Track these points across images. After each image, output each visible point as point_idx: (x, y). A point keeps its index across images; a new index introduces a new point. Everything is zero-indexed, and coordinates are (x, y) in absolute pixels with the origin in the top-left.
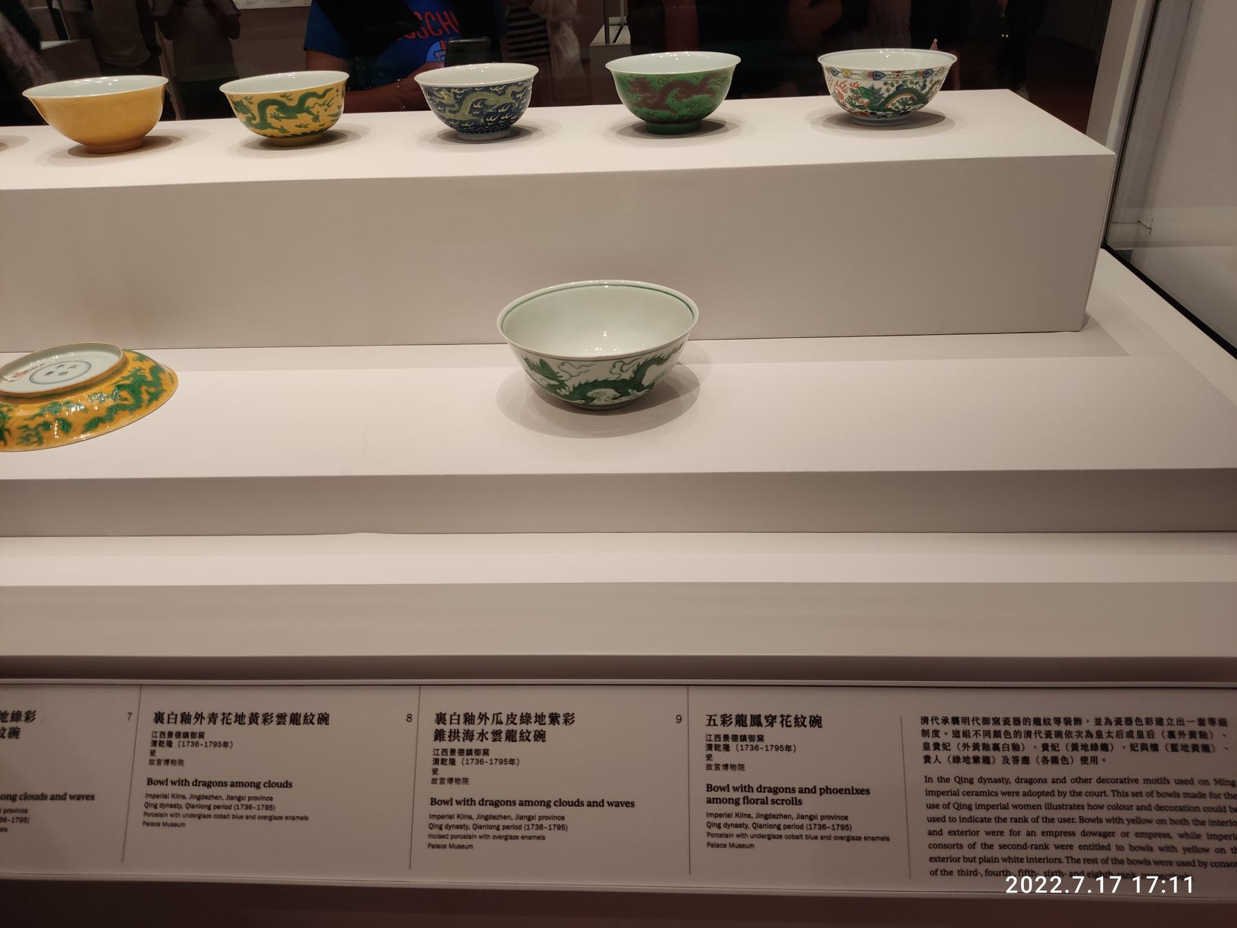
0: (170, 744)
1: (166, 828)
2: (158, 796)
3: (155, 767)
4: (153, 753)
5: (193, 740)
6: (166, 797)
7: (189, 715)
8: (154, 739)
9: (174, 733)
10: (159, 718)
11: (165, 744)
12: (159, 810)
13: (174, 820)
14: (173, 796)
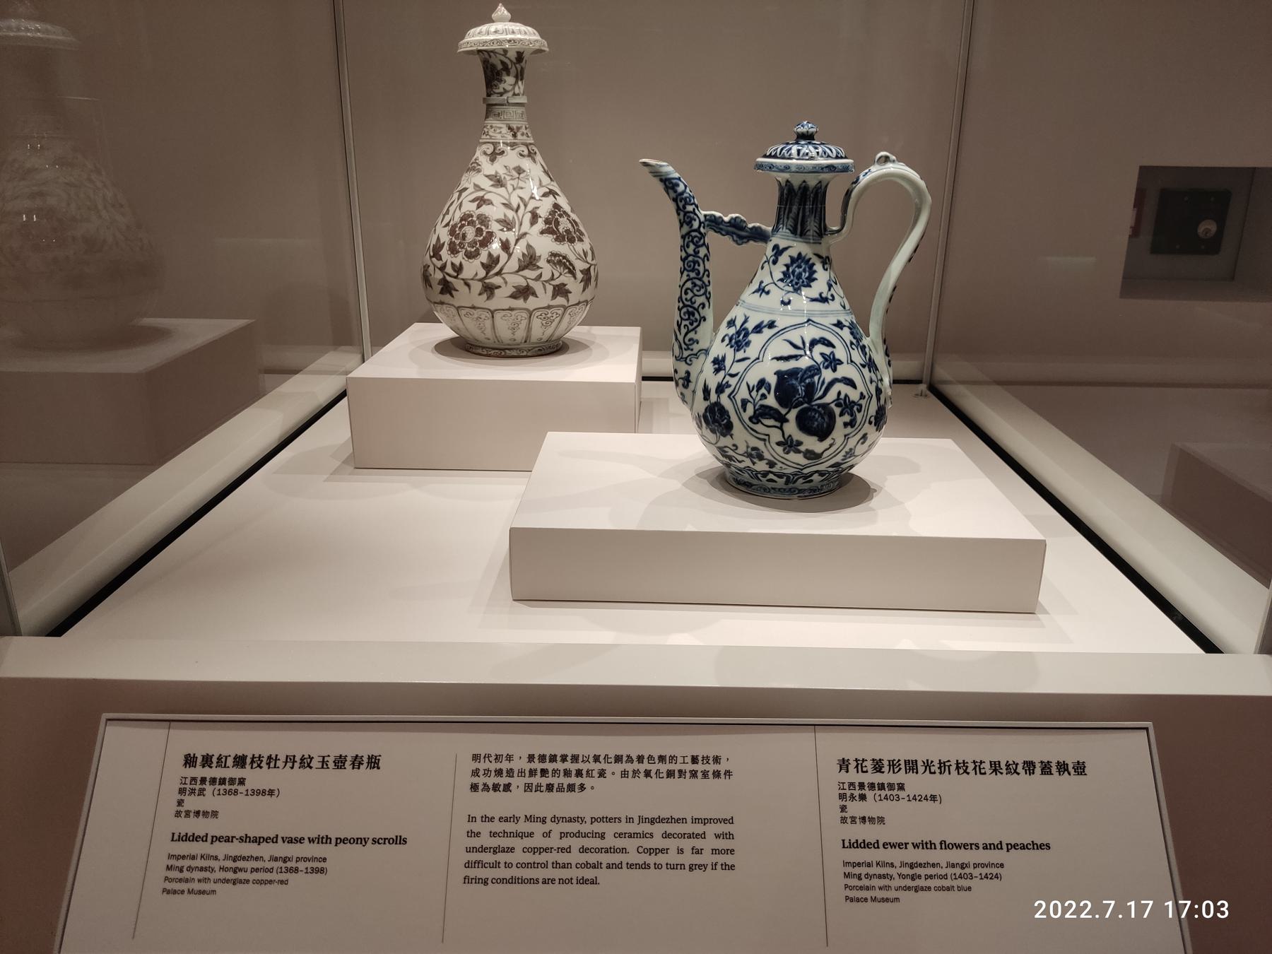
0: (201, 792)
2: (183, 857)
4: (180, 803)
5: (231, 787)
6: (193, 858)
7: (195, 757)
8: (183, 786)
9: (208, 780)
10: (190, 761)
12: (186, 874)
14: (202, 857)
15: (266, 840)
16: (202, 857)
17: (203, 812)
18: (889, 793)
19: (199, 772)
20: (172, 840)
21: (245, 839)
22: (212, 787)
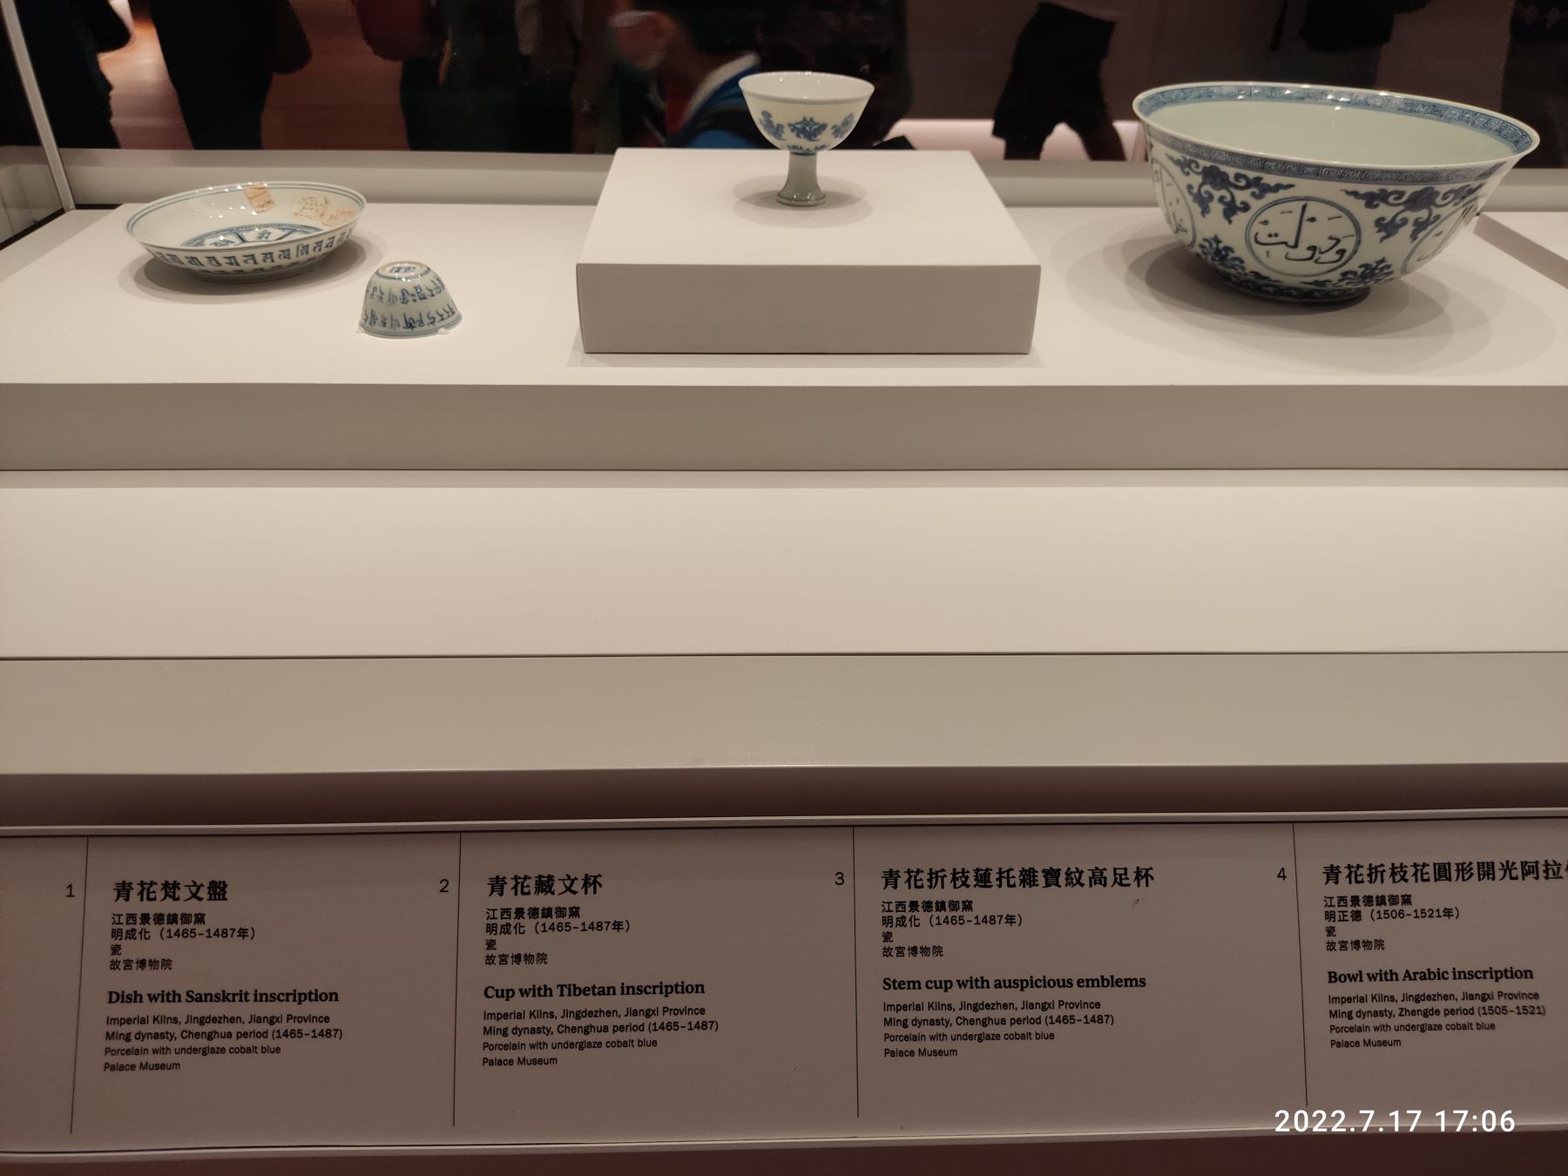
1: (525, 1067)
3: (497, 968)
9: (526, 911)
18: (950, 914)
21: (261, 997)
22: (534, 922)
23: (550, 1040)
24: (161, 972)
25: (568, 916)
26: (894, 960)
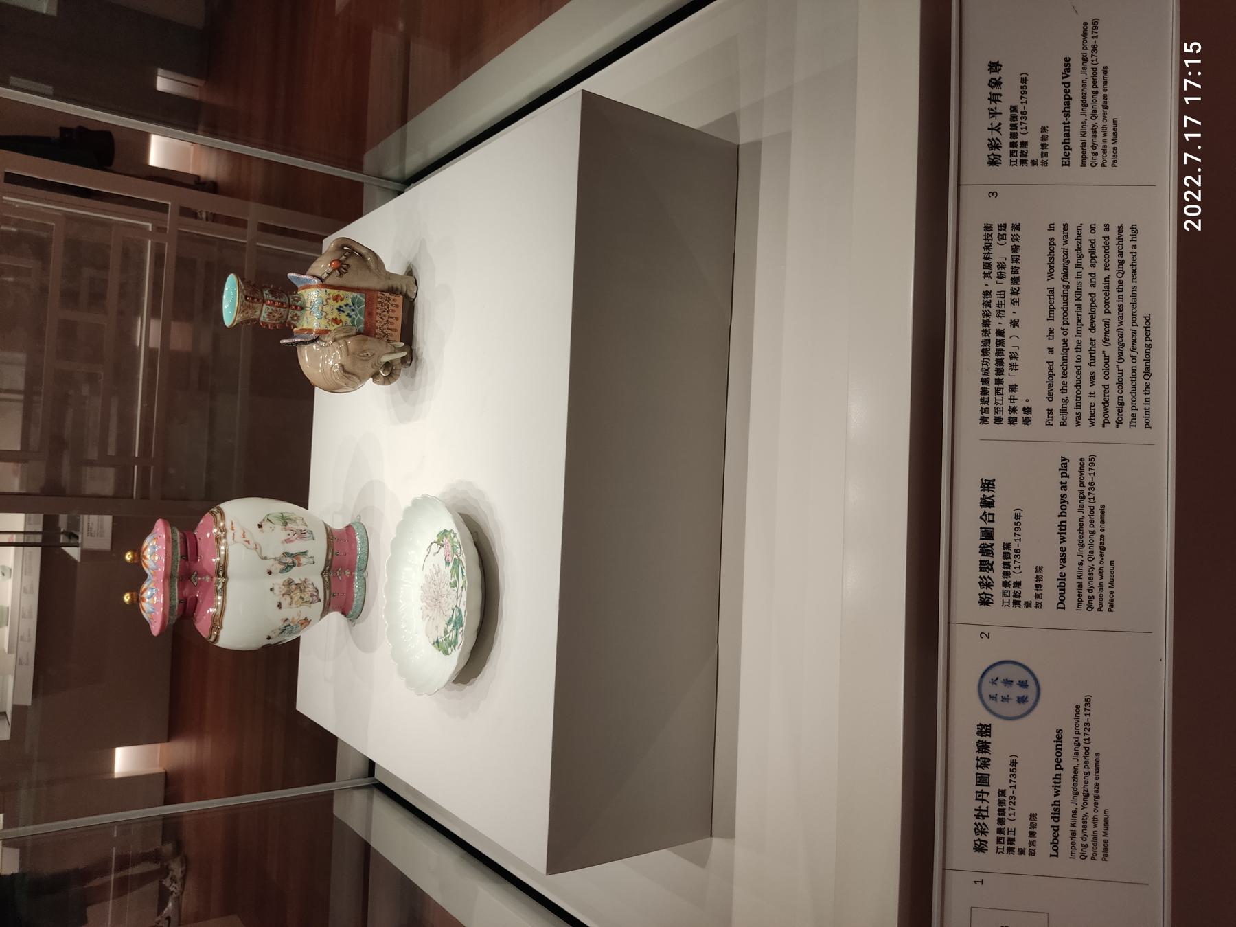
0: (1018, 584)
2: (1080, 596)
3: (1044, 601)
4: (1028, 605)
5: (1012, 556)
11: (1017, 590)
12: (1096, 593)
13: (1107, 574)
15: (1067, 92)
16: (1079, 578)
17: (1037, 581)
19: (997, 590)
20: (1064, 608)
23: (1097, 565)
24: (1039, 821)
25: (1009, 551)
26: (1050, 159)
